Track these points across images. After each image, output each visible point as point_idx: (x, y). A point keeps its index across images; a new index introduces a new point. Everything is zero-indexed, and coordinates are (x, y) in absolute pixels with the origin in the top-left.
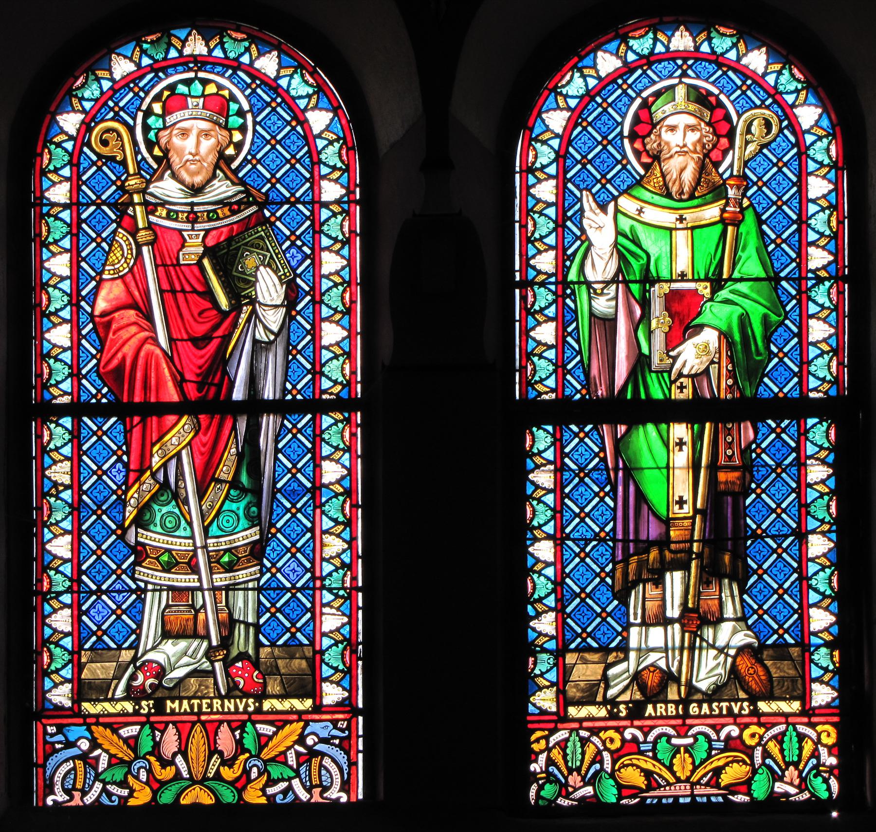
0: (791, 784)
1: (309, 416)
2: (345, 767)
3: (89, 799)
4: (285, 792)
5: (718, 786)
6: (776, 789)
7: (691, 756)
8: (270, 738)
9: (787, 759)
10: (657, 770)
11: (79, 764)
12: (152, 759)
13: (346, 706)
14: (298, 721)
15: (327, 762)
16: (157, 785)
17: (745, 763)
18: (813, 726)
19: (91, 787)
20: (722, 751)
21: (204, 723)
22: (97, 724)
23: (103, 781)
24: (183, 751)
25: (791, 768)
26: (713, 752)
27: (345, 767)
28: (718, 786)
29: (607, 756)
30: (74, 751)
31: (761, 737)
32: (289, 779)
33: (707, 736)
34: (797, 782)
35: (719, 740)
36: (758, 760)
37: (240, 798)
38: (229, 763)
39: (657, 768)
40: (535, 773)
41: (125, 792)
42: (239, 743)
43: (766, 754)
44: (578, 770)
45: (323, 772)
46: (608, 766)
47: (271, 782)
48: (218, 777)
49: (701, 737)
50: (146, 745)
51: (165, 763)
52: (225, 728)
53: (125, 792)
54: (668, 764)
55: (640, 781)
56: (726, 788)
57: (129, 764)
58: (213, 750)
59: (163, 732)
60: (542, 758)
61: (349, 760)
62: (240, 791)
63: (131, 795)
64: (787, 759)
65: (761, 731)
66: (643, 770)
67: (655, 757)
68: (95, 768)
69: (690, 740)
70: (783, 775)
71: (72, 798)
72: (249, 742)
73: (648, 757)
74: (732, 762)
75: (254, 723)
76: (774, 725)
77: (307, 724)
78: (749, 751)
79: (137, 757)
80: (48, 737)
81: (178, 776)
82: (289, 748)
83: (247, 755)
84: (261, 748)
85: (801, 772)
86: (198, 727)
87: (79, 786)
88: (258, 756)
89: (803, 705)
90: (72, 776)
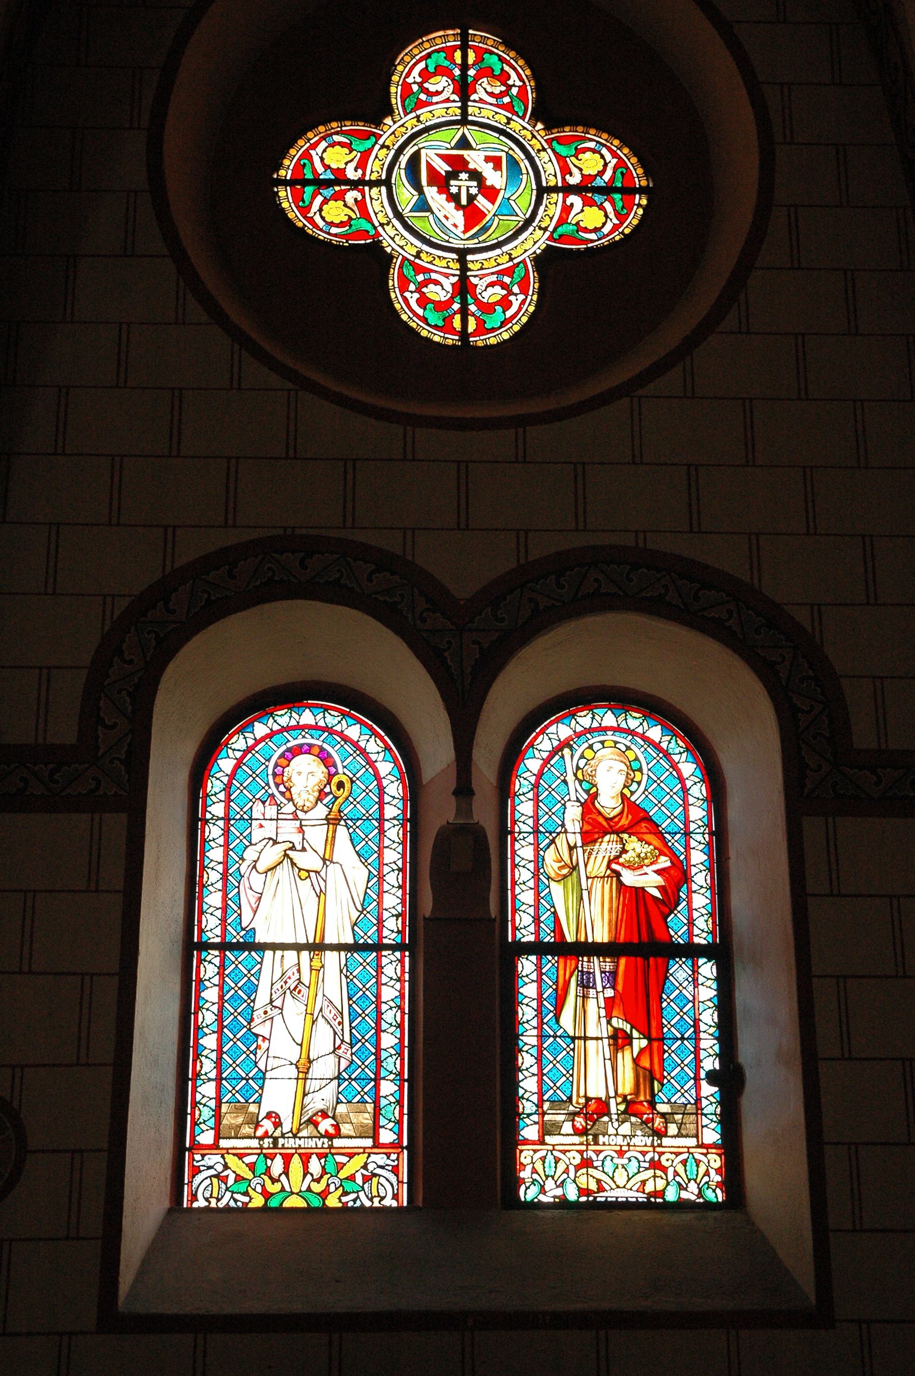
1: (374, 954)
2: (395, 1184)
3: (221, 1205)
4: (354, 1201)
5: (644, 1192)
6: (682, 1196)
7: (626, 1170)
8: (345, 1164)
11: (215, 1180)
12: (266, 1178)
13: (396, 1145)
14: (364, 1153)
15: (382, 1180)
16: (267, 1195)
17: (662, 1178)
18: (705, 1155)
19: (222, 1197)
20: (647, 1169)
21: (300, 1155)
22: (228, 1153)
23: (233, 1192)
24: (286, 1172)
26: (641, 1169)
27: (395, 1184)
29: (572, 1169)
30: (212, 1172)
31: (673, 1161)
32: (358, 1192)
33: (636, 1158)
34: (696, 1191)
35: (645, 1161)
36: (670, 1177)
37: (324, 1203)
38: (318, 1181)
40: (524, 1179)
41: (246, 1199)
42: (323, 1168)
43: (676, 1174)
44: (553, 1177)
45: (380, 1186)
47: (345, 1193)
48: (309, 1189)
50: (260, 1168)
51: (274, 1181)
52: (314, 1157)
53: (246, 1199)
54: (611, 1176)
55: (593, 1186)
57: (250, 1181)
58: (306, 1172)
59: (272, 1160)
60: (529, 1169)
61: (398, 1180)
62: (324, 1200)
63: (250, 1201)
64: (689, 1177)
65: (673, 1156)
67: (603, 1171)
68: (226, 1184)
70: (687, 1187)
71: (210, 1203)
72: (330, 1168)
75: (333, 1154)
76: (681, 1153)
77: (369, 1156)
78: (664, 1170)
79: (255, 1177)
80: (195, 1163)
81: (283, 1189)
82: (357, 1171)
83: (329, 1175)
84: (338, 1172)
85: (699, 1185)
86: (296, 1156)
87: (215, 1195)
88: (336, 1176)
89: (698, 1141)
90: (210, 1189)
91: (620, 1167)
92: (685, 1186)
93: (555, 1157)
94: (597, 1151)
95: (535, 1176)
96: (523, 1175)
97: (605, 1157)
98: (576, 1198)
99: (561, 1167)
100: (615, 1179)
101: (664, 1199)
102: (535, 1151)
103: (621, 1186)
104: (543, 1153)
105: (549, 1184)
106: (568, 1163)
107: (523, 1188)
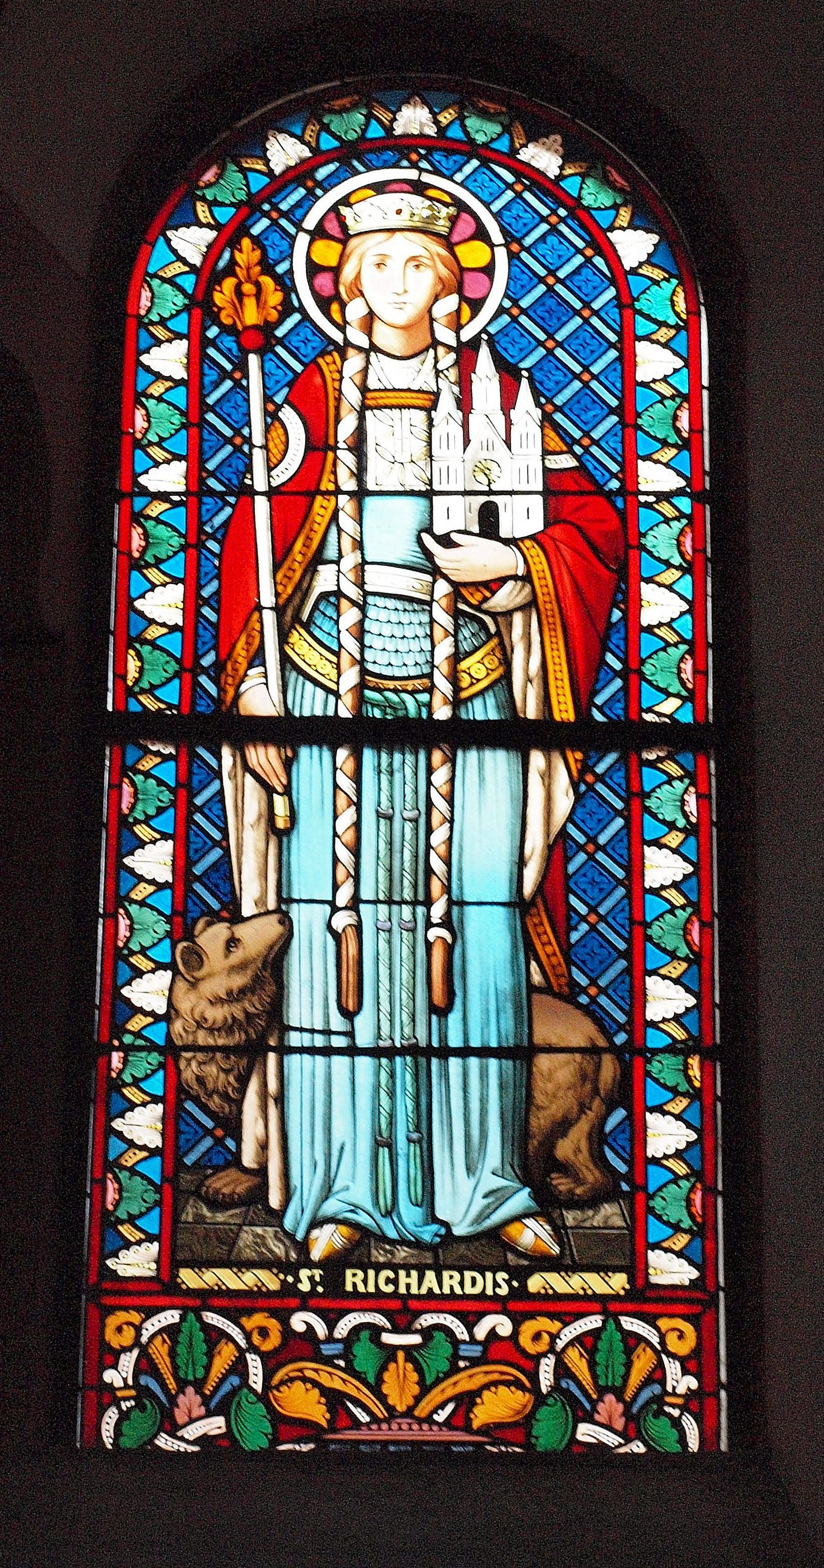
0: (609, 1427)
5: (467, 1428)
6: (580, 1437)
7: (418, 1369)
9: (602, 1382)
10: (354, 1392)
20: (474, 1362)
25: (610, 1398)
28: (467, 1428)
31: (554, 1337)
34: (619, 1424)
36: (546, 1378)
39: (352, 1387)
43: (562, 1370)
46: (256, 1381)
49: (439, 1336)
55: (319, 1414)
56: (485, 1430)
64: (602, 1382)
66: (325, 1392)
67: (350, 1370)
69: (416, 1339)
70: (594, 1409)
73: (338, 1367)
74: (496, 1383)
91: (401, 1355)
92: (587, 1406)
93: (207, 1328)
94: (330, 1310)
95: (144, 1380)
96: (110, 1376)
97: (357, 1330)
98: (264, 1443)
99: (225, 1355)
100: (385, 1389)
101: (529, 1446)
102: (150, 1312)
103: (401, 1408)
104: (171, 1317)
105: (189, 1400)
106: (243, 1343)
107: (111, 1416)
